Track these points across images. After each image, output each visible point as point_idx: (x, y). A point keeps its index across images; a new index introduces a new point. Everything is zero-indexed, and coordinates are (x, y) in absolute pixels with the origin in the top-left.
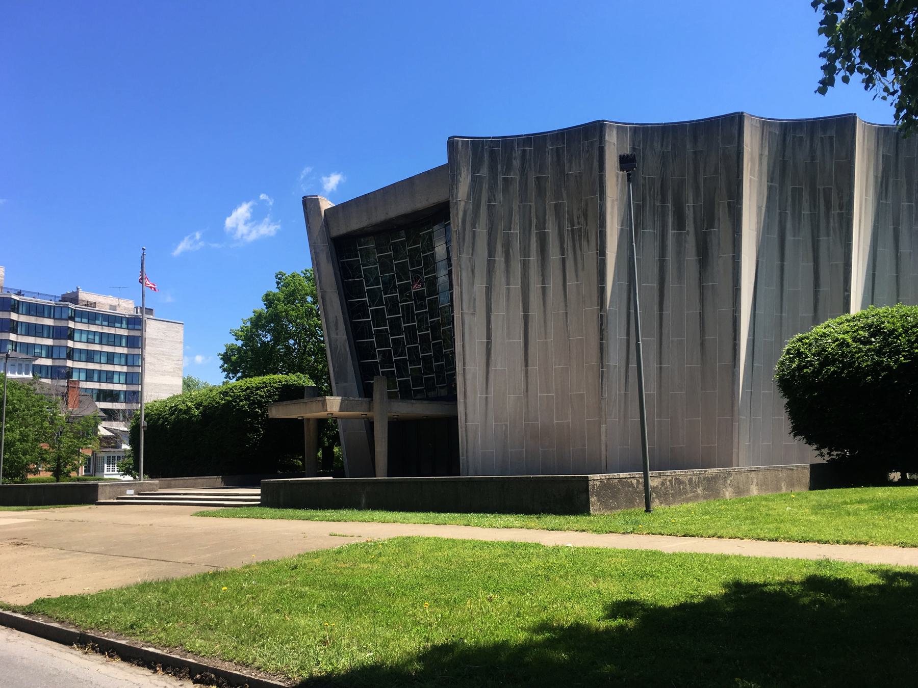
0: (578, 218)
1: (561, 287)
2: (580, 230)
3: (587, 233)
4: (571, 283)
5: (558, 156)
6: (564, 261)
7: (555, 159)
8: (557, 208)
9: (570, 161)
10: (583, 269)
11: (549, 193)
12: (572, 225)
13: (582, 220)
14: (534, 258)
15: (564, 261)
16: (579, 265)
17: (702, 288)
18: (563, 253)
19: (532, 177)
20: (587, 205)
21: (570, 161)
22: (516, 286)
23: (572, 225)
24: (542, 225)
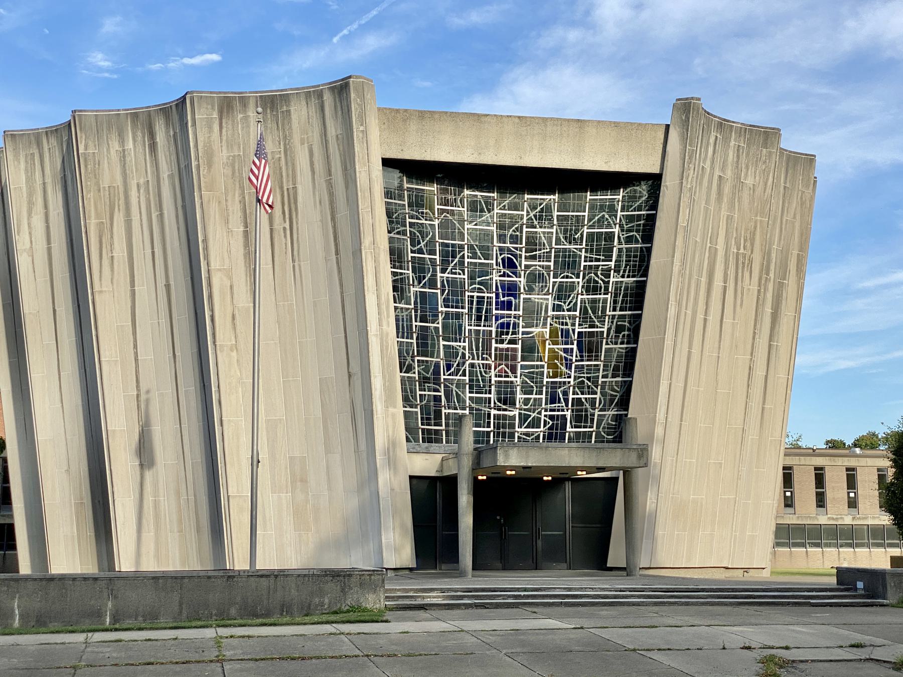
0: (745, 241)
1: (719, 324)
2: (744, 256)
3: (751, 261)
4: (727, 320)
5: (738, 156)
6: (725, 287)
7: (735, 160)
8: (729, 219)
9: (747, 167)
10: (741, 305)
11: (725, 200)
12: (738, 249)
13: (748, 244)
14: (704, 280)
15: (725, 287)
16: (739, 302)
17: (770, 346)
18: (725, 282)
19: (717, 173)
20: (755, 227)
21: (747, 167)
22: (689, 312)
23: (738, 249)
24: (714, 239)
